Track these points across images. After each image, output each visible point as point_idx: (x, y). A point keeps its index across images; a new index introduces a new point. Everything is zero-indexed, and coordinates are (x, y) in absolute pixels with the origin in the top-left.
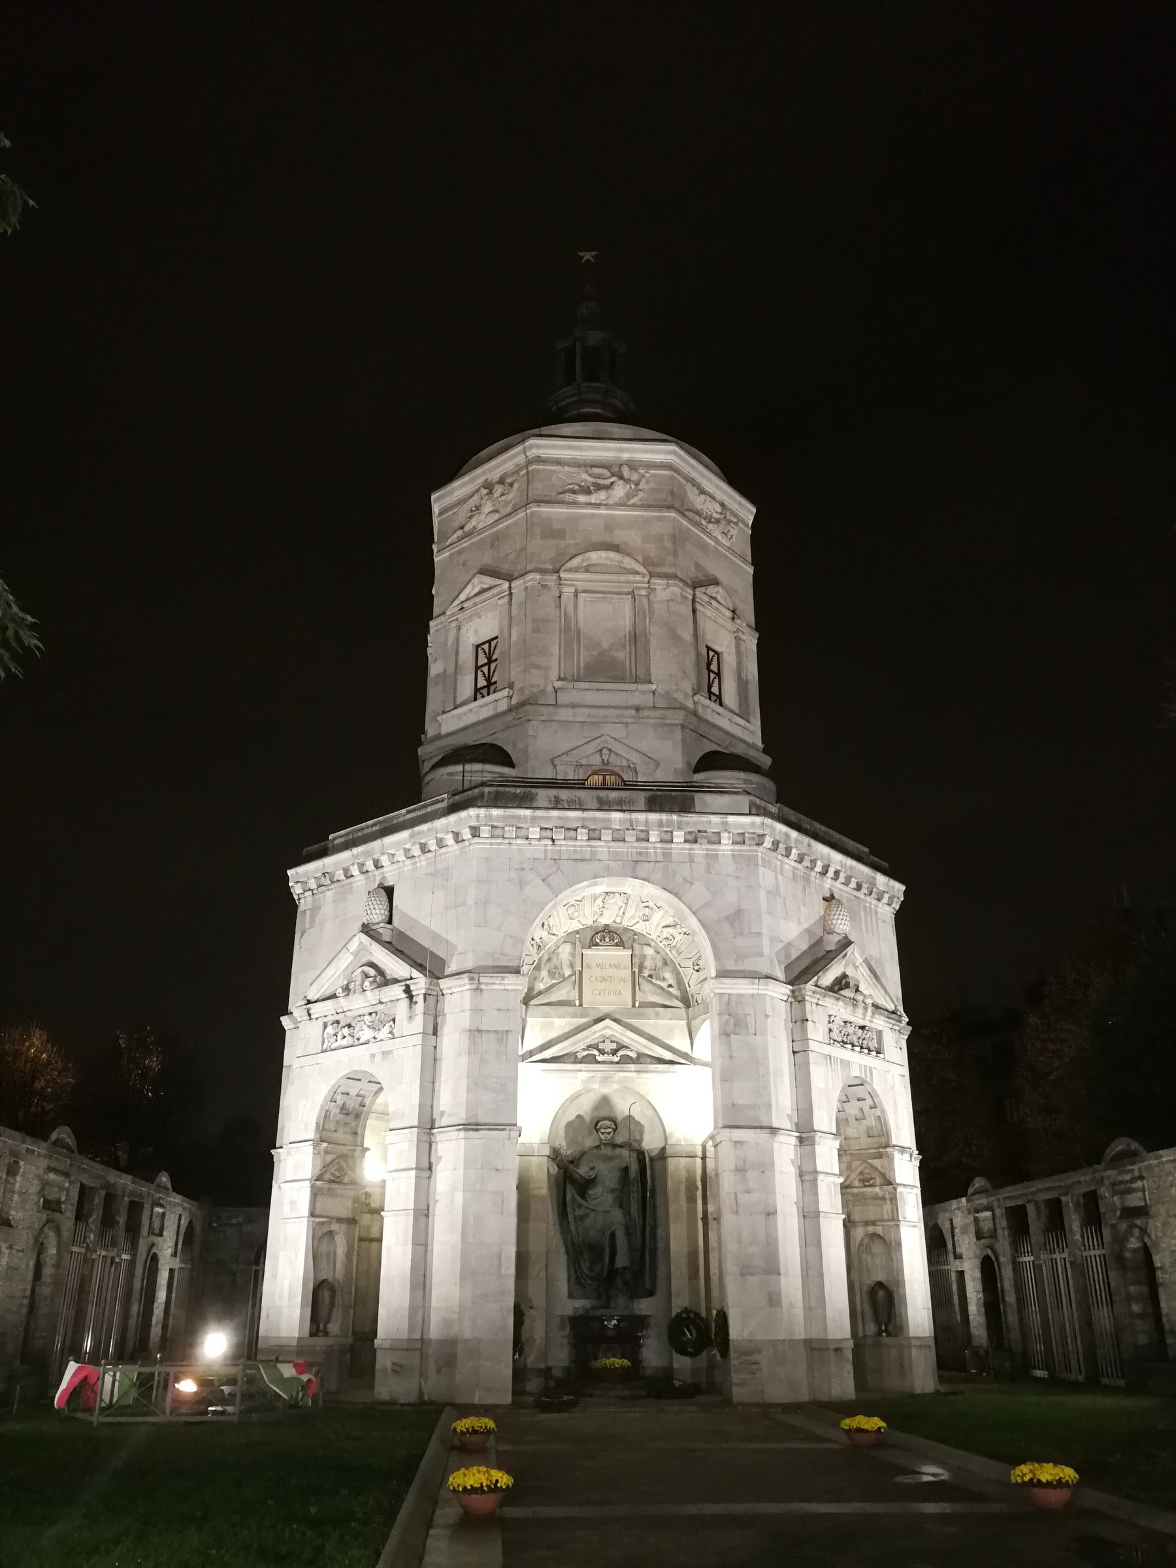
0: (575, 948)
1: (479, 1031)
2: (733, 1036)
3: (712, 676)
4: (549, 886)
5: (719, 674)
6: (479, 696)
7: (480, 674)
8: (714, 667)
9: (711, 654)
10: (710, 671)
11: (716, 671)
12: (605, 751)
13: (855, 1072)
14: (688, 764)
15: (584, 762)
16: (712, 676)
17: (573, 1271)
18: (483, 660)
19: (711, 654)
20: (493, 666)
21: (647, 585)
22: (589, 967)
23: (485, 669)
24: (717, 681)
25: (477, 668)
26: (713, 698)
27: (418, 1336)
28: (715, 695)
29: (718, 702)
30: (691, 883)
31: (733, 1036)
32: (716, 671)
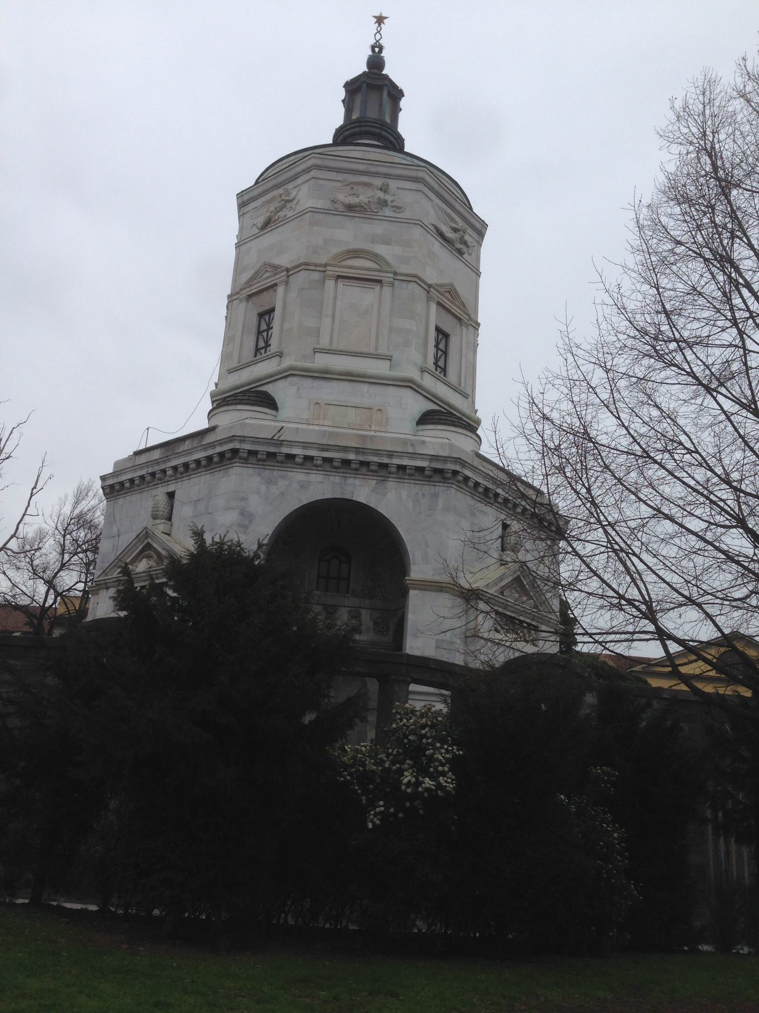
5: (445, 353)
6: (258, 354)
7: (260, 337)
8: (442, 346)
11: (444, 349)
16: (440, 353)
18: (264, 327)
19: (440, 337)
20: (270, 332)
23: (265, 334)
24: (443, 357)
26: (439, 369)
28: (440, 367)
29: (443, 373)
32: (444, 349)
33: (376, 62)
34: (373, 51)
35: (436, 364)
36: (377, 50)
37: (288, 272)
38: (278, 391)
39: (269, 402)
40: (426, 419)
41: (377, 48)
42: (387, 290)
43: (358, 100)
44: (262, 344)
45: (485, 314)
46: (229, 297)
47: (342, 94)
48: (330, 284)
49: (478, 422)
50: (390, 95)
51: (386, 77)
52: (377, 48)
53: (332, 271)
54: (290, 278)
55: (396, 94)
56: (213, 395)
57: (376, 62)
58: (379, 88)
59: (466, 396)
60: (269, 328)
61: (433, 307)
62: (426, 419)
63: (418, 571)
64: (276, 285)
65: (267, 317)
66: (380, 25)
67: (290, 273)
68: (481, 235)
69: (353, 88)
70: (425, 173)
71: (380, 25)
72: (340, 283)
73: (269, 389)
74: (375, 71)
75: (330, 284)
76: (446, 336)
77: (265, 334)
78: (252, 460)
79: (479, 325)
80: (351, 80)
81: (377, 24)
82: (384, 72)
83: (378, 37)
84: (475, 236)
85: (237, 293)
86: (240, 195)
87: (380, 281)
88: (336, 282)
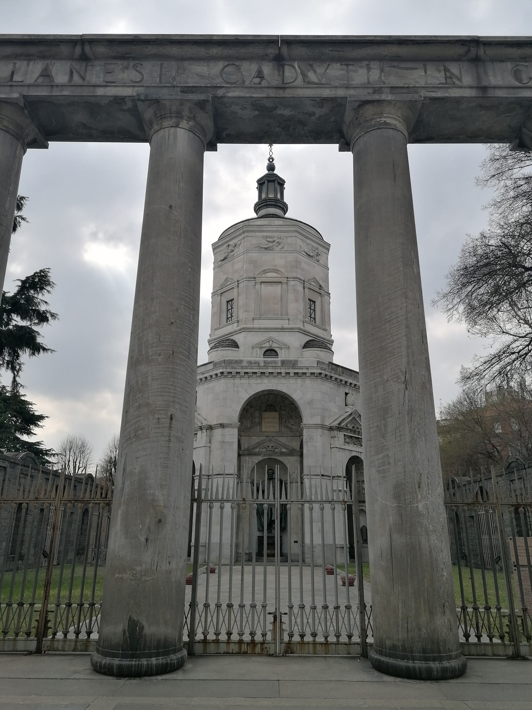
0: (260, 412)
1: (223, 442)
2: (309, 443)
3: (312, 311)
4: (247, 393)
5: (314, 310)
6: (228, 320)
7: (228, 312)
8: (312, 308)
9: (312, 303)
10: (311, 309)
12: (271, 342)
13: (354, 454)
14: (300, 345)
15: (263, 346)
16: (312, 311)
17: (259, 522)
18: (230, 307)
21: (288, 279)
22: (264, 418)
24: (314, 312)
25: (228, 310)
26: (312, 319)
27: (204, 542)
29: (314, 321)
30: (296, 391)
31: (309, 443)
33: (271, 167)
34: (269, 161)
35: (310, 317)
36: (271, 160)
37: (238, 281)
38: (239, 338)
39: (235, 345)
40: (307, 345)
41: (271, 159)
42: (285, 286)
43: (265, 187)
44: (229, 316)
45: (332, 289)
46: (212, 293)
47: (256, 185)
48: (258, 286)
49: (332, 342)
50: (279, 183)
51: (277, 176)
52: (271, 159)
53: (259, 280)
54: (239, 285)
55: (281, 183)
56: (210, 342)
57: (271, 167)
58: (273, 181)
59: (325, 330)
60: (232, 308)
61: (306, 290)
62: (307, 345)
63: (307, 420)
64: (233, 288)
65: (231, 302)
66: (271, 146)
67: (239, 282)
68: (328, 250)
69: (261, 183)
70: (297, 228)
71: (271, 146)
72: (263, 285)
73: (235, 338)
74: (271, 172)
75: (258, 286)
76: (314, 302)
77: (230, 311)
78: (230, 376)
79: (330, 294)
80: (260, 179)
81: (270, 147)
82: (275, 172)
83: (271, 154)
84: (324, 250)
85: (217, 291)
86: (213, 245)
87: (281, 282)
88: (261, 285)
